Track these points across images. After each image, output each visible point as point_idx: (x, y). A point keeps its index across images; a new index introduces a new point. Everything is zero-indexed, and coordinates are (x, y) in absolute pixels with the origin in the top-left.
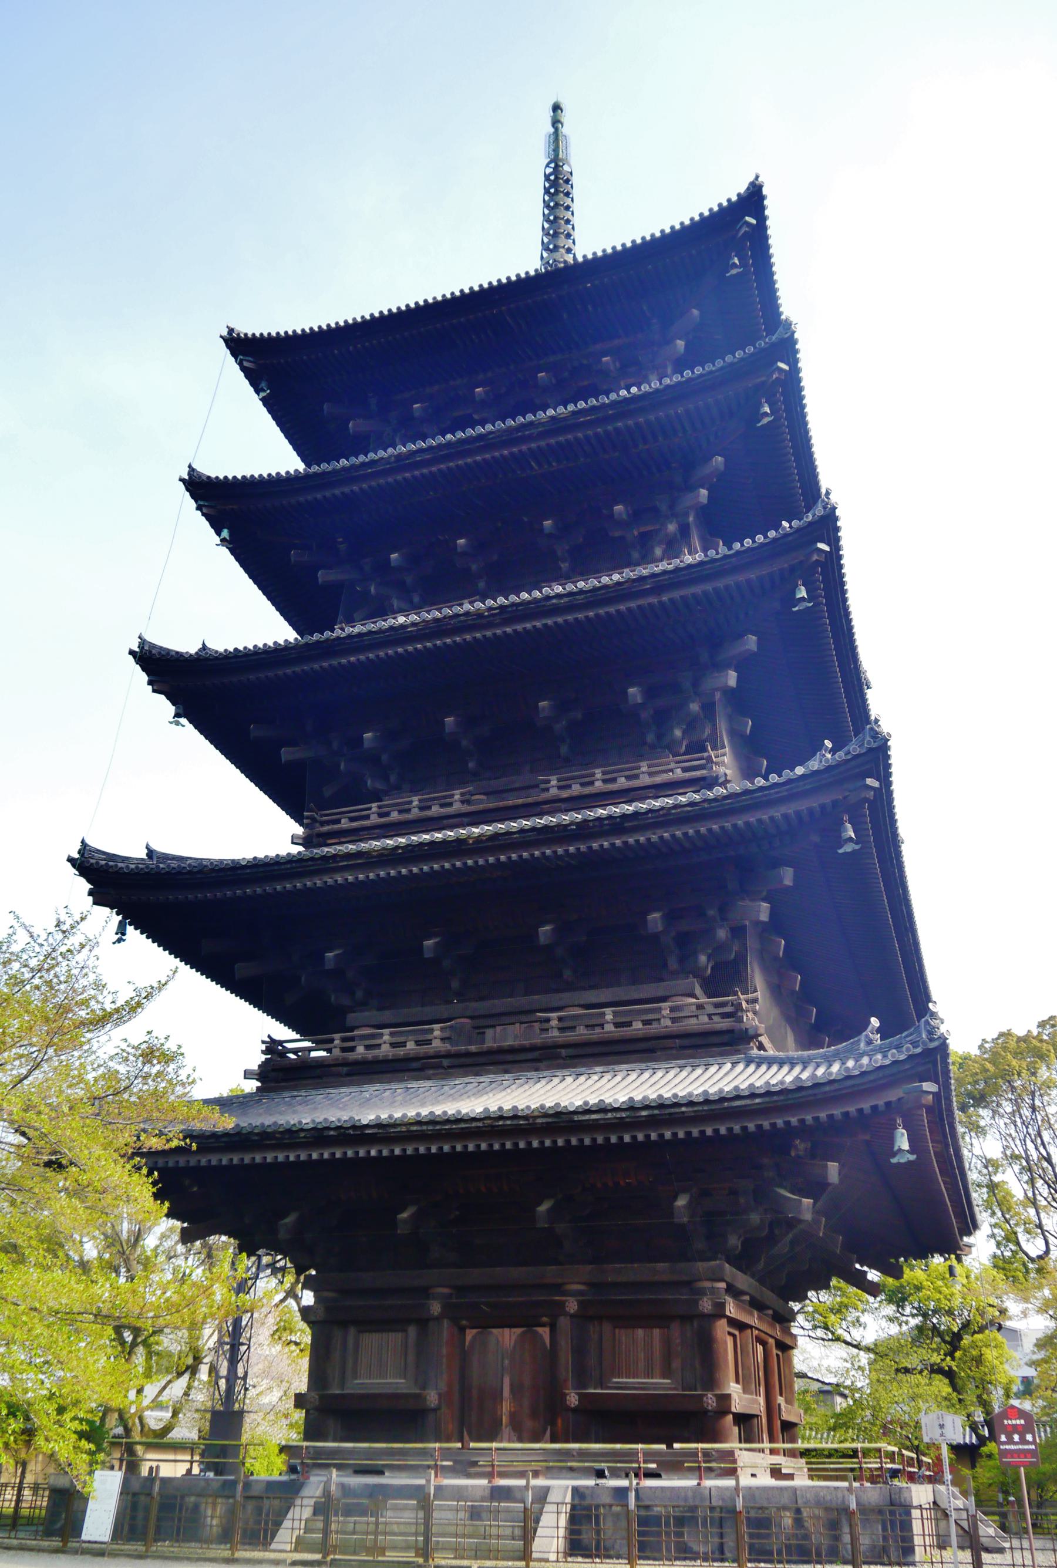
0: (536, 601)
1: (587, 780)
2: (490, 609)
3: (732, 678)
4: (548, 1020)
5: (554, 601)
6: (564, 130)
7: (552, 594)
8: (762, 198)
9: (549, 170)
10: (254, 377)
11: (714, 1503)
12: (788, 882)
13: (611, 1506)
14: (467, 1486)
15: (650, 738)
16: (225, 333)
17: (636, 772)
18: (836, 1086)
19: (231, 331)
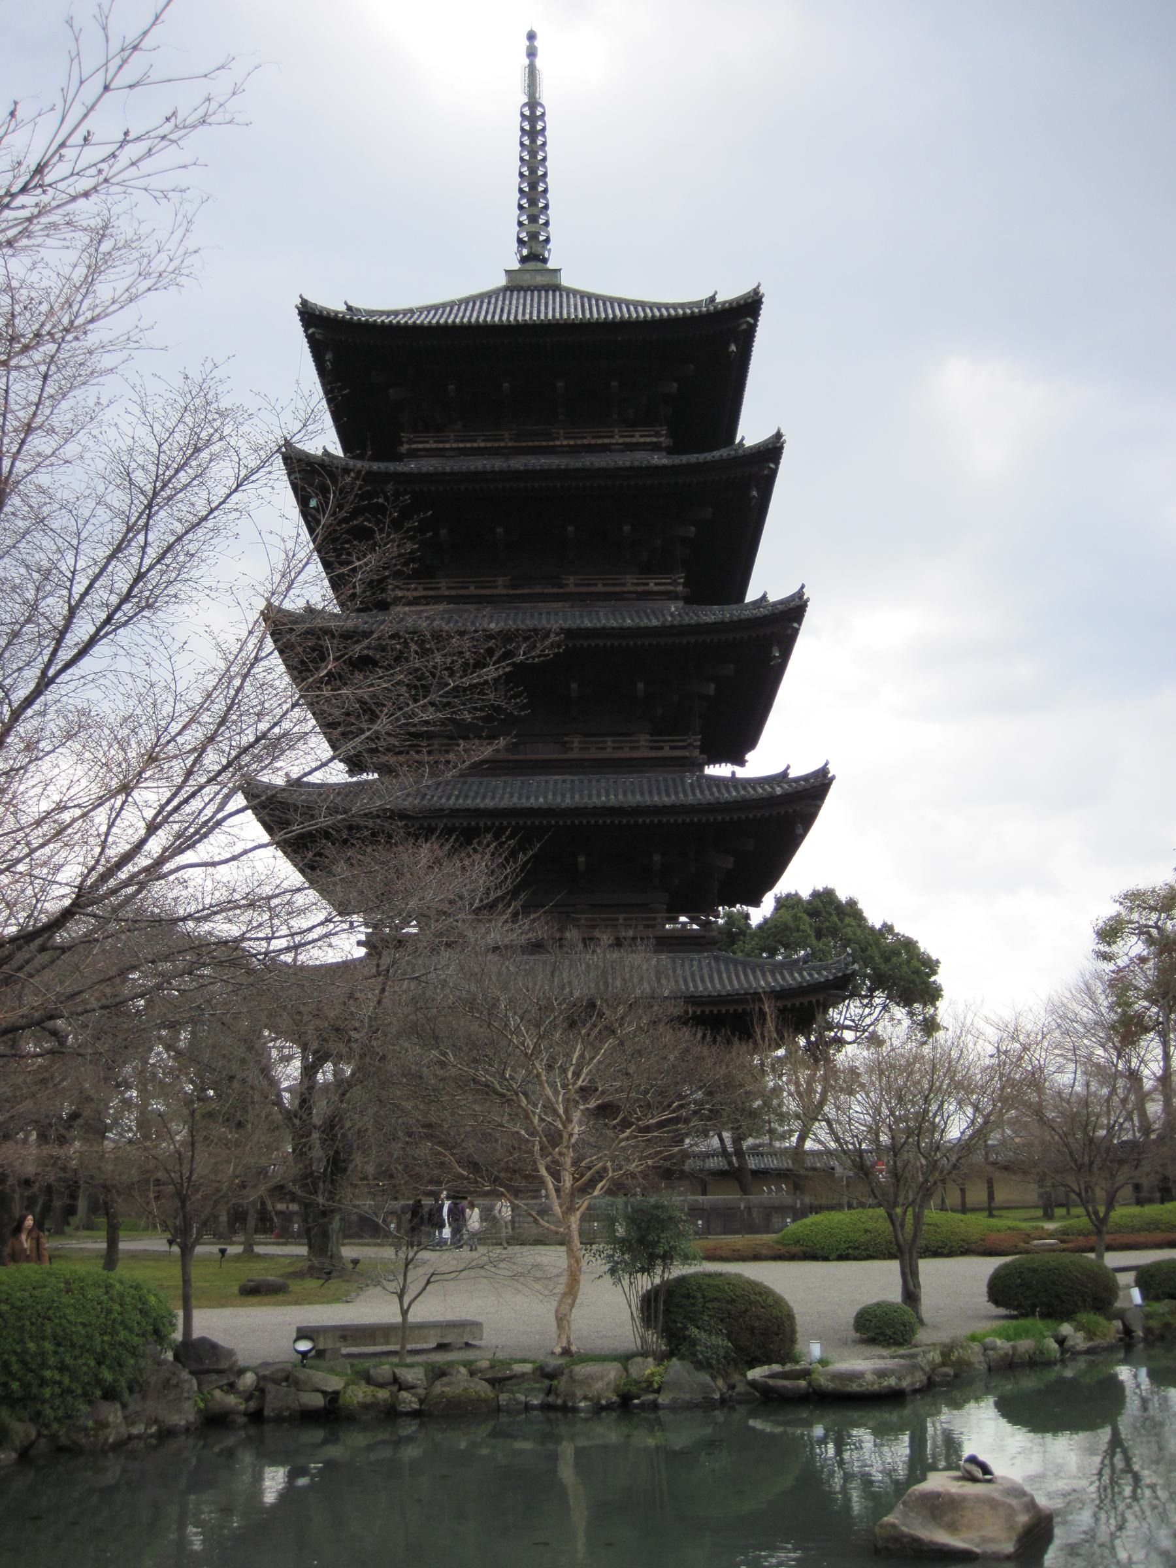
3: (711, 689)
4: (578, 919)
6: (539, 62)
8: (761, 303)
19: (304, 302)
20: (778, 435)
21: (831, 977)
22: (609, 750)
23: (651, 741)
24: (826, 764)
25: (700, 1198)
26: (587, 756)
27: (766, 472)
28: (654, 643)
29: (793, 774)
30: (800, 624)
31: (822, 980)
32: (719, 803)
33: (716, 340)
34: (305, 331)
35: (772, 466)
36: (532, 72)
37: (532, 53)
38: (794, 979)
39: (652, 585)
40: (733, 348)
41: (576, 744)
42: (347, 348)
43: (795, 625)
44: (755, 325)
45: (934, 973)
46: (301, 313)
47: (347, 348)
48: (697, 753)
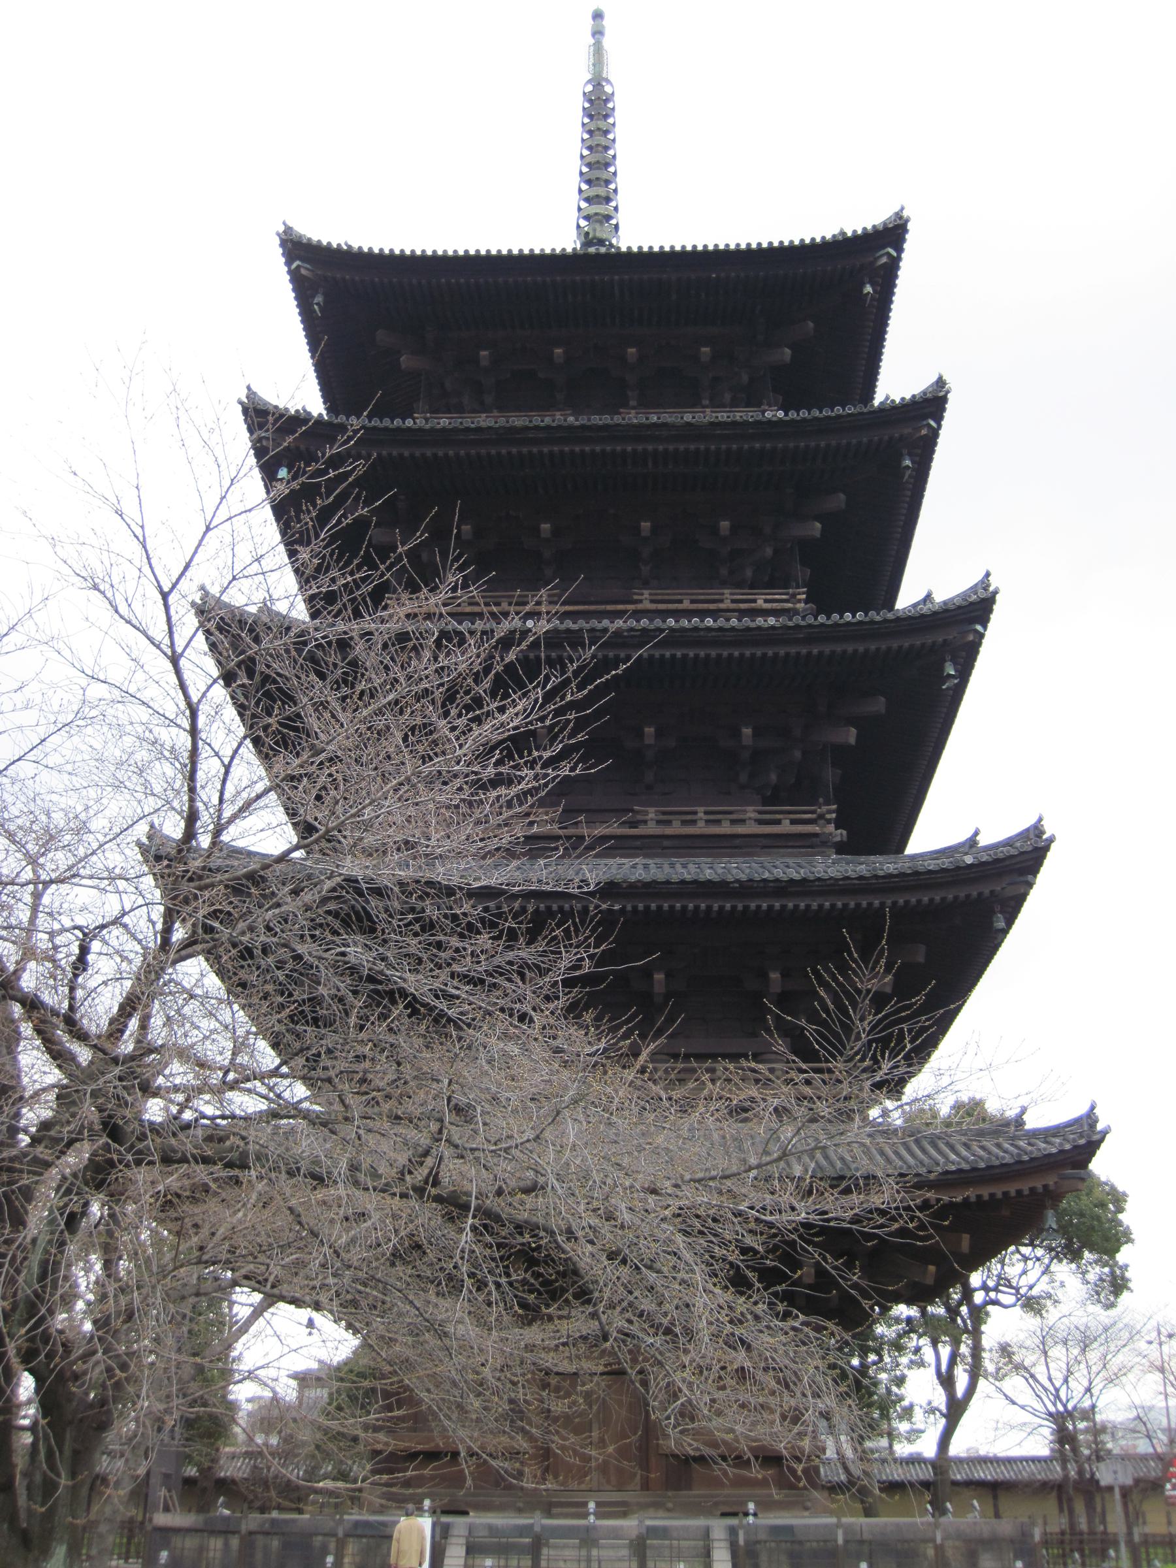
0: (683, 630)
1: (689, 817)
2: (632, 629)
5: (702, 633)
6: (607, 42)
7: (702, 626)
8: (906, 231)
9: (589, 88)
10: (303, 288)
11: (866, 1536)
12: (921, 959)
13: (765, 1542)
14: (622, 1527)
15: (743, 778)
16: (281, 229)
17: (742, 817)
18: (1005, 1170)
19: (288, 230)
20: (940, 383)
21: (1068, 1147)
22: (701, 824)
23: (760, 813)
24: (1040, 819)
25: (863, 1520)
26: (669, 831)
27: (924, 432)
28: (770, 653)
29: (984, 841)
30: (985, 628)
31: (1054, 1150)
32: (876, 877)
33: (850, 279)
34: (288, 263)
35: (932, 423)
36: (598, 52)
37: (598, 33)
38: (1006, 1151)
39: (760, 602)
40: (868, 289)
41: (652, 816)
42: (343, 292)
43: (979, 628)
44: (898, 259)
45: (1120, 1210)
46: (283, 243)
47: (343, 292)
48: (831, 828)
